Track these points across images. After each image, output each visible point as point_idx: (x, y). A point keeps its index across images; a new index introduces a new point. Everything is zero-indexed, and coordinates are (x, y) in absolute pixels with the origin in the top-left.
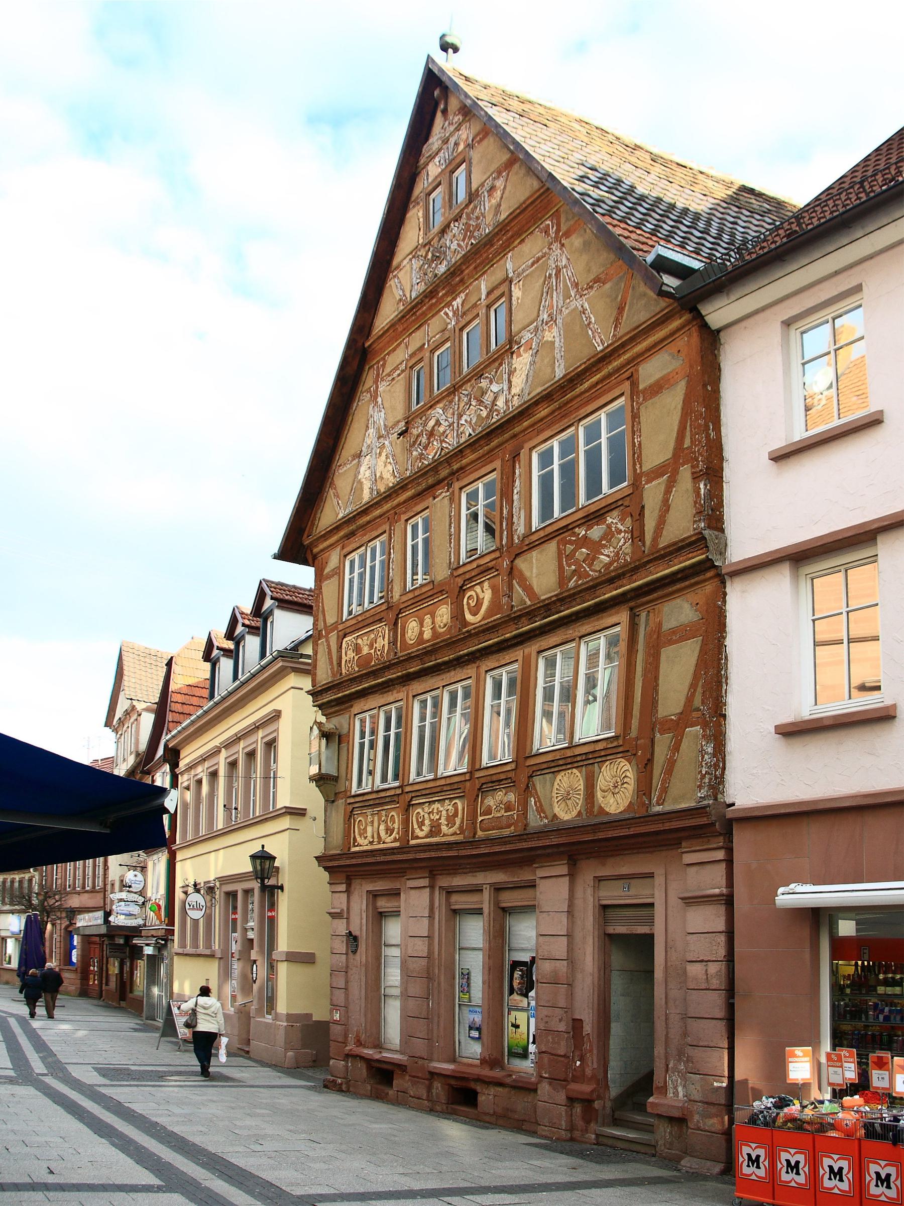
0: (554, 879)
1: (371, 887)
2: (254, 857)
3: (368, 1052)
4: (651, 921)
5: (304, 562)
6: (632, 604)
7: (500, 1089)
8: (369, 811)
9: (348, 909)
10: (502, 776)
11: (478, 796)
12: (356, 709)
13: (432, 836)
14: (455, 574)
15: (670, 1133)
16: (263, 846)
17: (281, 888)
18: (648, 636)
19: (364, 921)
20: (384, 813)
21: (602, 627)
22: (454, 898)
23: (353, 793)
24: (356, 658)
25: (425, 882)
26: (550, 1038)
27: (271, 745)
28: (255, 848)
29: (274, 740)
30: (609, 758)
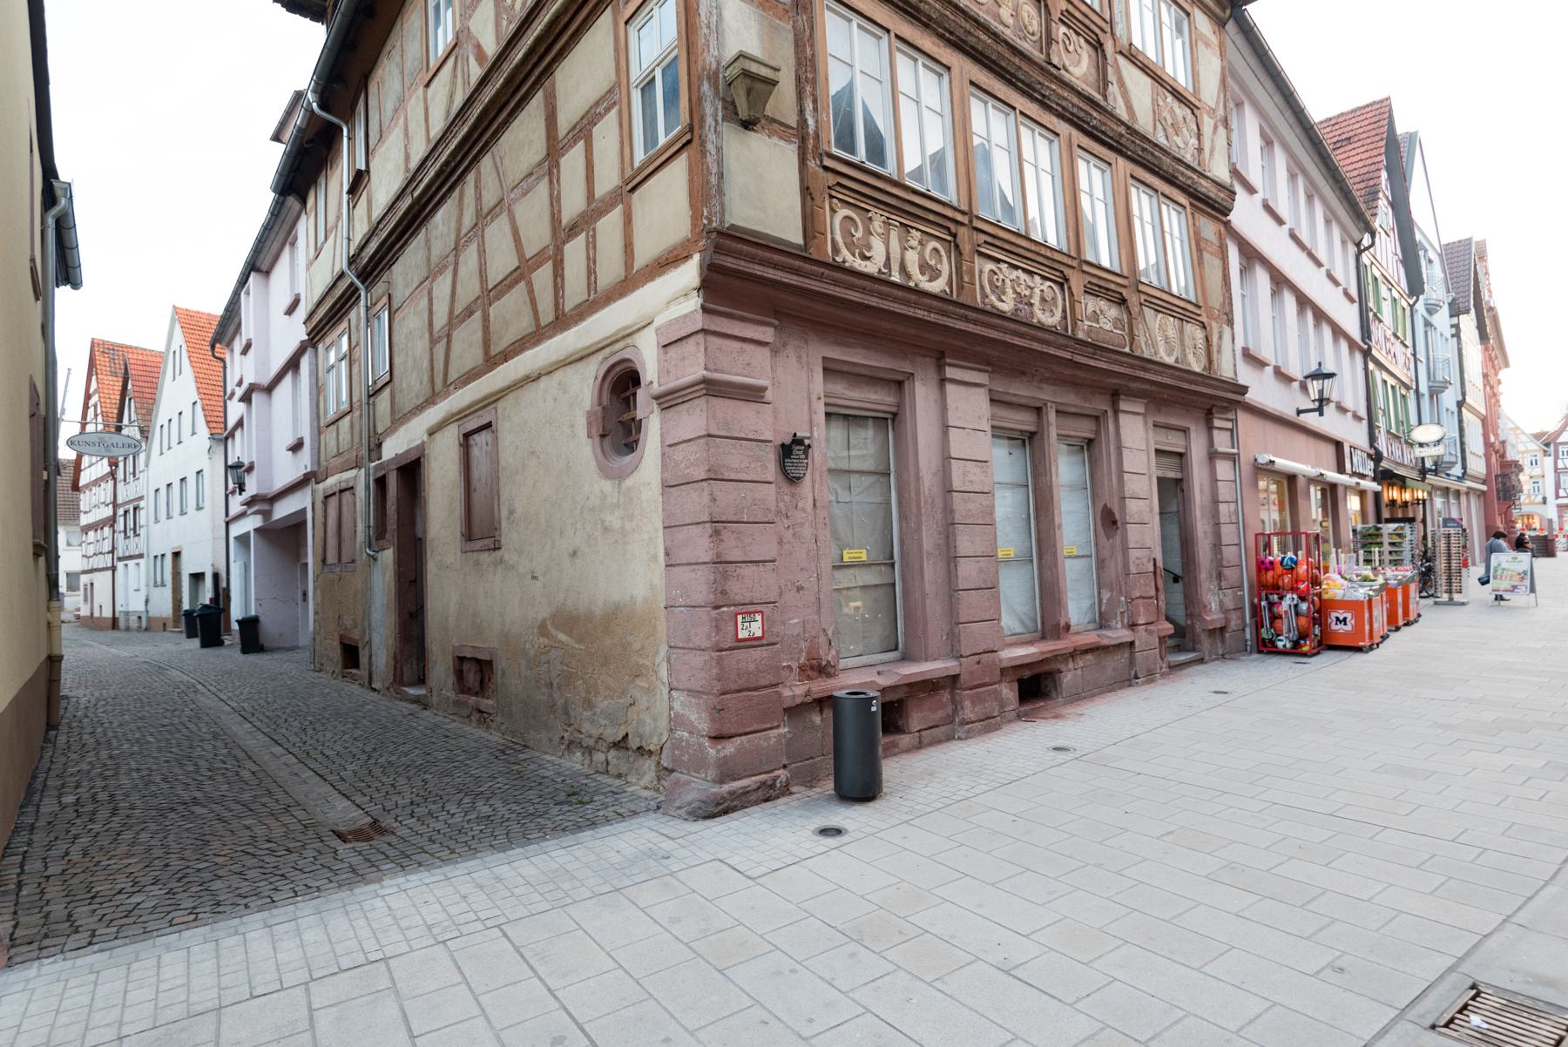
10: (1112, 286)
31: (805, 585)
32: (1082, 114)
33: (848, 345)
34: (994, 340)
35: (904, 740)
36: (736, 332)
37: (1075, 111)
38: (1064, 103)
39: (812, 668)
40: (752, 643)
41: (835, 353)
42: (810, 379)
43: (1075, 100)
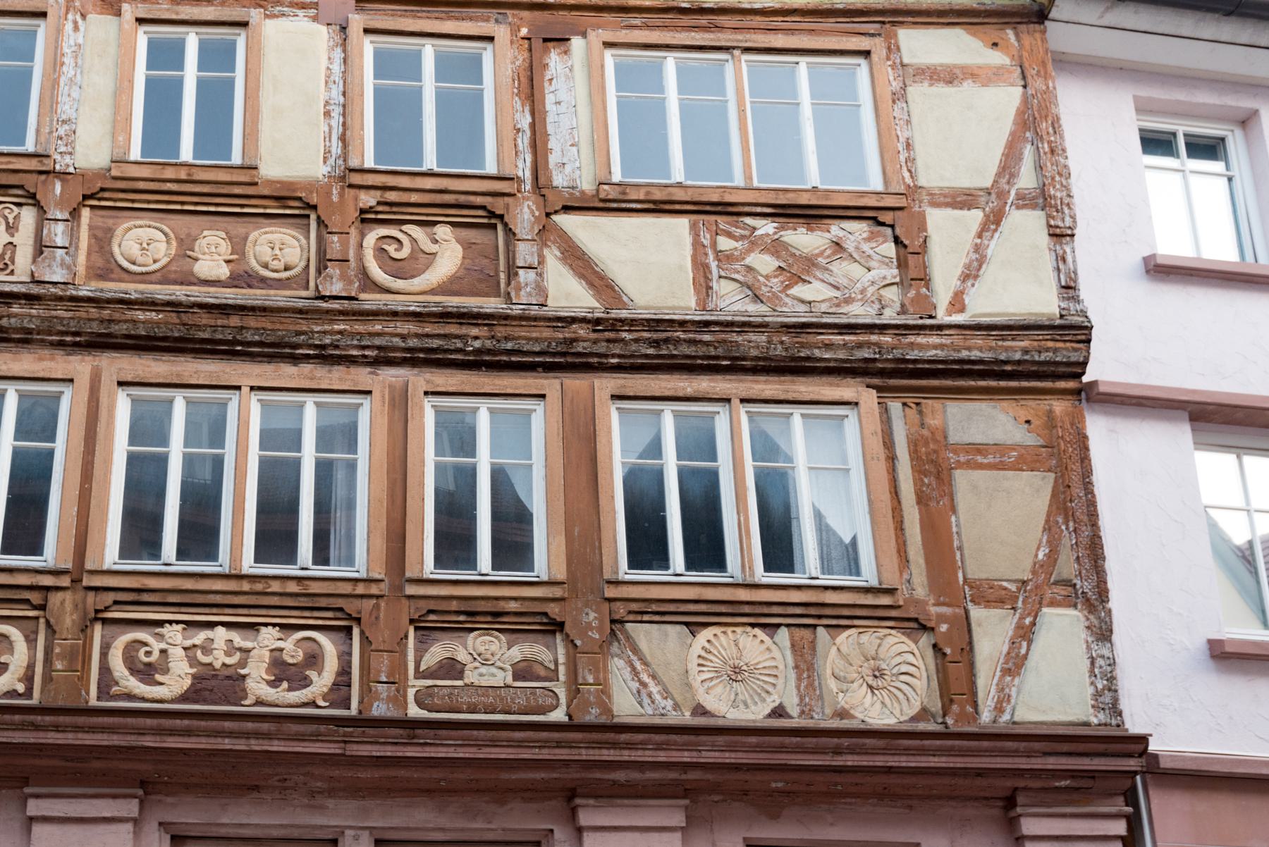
10: (513, 606)
13: (196, 702)
14: (356, 179)
21: (807, 398)
25: (130, 808)
30: (856, 622)
32: (435, 343)
34: (119, 749)
37: (413, 343)
38: (377, 341)
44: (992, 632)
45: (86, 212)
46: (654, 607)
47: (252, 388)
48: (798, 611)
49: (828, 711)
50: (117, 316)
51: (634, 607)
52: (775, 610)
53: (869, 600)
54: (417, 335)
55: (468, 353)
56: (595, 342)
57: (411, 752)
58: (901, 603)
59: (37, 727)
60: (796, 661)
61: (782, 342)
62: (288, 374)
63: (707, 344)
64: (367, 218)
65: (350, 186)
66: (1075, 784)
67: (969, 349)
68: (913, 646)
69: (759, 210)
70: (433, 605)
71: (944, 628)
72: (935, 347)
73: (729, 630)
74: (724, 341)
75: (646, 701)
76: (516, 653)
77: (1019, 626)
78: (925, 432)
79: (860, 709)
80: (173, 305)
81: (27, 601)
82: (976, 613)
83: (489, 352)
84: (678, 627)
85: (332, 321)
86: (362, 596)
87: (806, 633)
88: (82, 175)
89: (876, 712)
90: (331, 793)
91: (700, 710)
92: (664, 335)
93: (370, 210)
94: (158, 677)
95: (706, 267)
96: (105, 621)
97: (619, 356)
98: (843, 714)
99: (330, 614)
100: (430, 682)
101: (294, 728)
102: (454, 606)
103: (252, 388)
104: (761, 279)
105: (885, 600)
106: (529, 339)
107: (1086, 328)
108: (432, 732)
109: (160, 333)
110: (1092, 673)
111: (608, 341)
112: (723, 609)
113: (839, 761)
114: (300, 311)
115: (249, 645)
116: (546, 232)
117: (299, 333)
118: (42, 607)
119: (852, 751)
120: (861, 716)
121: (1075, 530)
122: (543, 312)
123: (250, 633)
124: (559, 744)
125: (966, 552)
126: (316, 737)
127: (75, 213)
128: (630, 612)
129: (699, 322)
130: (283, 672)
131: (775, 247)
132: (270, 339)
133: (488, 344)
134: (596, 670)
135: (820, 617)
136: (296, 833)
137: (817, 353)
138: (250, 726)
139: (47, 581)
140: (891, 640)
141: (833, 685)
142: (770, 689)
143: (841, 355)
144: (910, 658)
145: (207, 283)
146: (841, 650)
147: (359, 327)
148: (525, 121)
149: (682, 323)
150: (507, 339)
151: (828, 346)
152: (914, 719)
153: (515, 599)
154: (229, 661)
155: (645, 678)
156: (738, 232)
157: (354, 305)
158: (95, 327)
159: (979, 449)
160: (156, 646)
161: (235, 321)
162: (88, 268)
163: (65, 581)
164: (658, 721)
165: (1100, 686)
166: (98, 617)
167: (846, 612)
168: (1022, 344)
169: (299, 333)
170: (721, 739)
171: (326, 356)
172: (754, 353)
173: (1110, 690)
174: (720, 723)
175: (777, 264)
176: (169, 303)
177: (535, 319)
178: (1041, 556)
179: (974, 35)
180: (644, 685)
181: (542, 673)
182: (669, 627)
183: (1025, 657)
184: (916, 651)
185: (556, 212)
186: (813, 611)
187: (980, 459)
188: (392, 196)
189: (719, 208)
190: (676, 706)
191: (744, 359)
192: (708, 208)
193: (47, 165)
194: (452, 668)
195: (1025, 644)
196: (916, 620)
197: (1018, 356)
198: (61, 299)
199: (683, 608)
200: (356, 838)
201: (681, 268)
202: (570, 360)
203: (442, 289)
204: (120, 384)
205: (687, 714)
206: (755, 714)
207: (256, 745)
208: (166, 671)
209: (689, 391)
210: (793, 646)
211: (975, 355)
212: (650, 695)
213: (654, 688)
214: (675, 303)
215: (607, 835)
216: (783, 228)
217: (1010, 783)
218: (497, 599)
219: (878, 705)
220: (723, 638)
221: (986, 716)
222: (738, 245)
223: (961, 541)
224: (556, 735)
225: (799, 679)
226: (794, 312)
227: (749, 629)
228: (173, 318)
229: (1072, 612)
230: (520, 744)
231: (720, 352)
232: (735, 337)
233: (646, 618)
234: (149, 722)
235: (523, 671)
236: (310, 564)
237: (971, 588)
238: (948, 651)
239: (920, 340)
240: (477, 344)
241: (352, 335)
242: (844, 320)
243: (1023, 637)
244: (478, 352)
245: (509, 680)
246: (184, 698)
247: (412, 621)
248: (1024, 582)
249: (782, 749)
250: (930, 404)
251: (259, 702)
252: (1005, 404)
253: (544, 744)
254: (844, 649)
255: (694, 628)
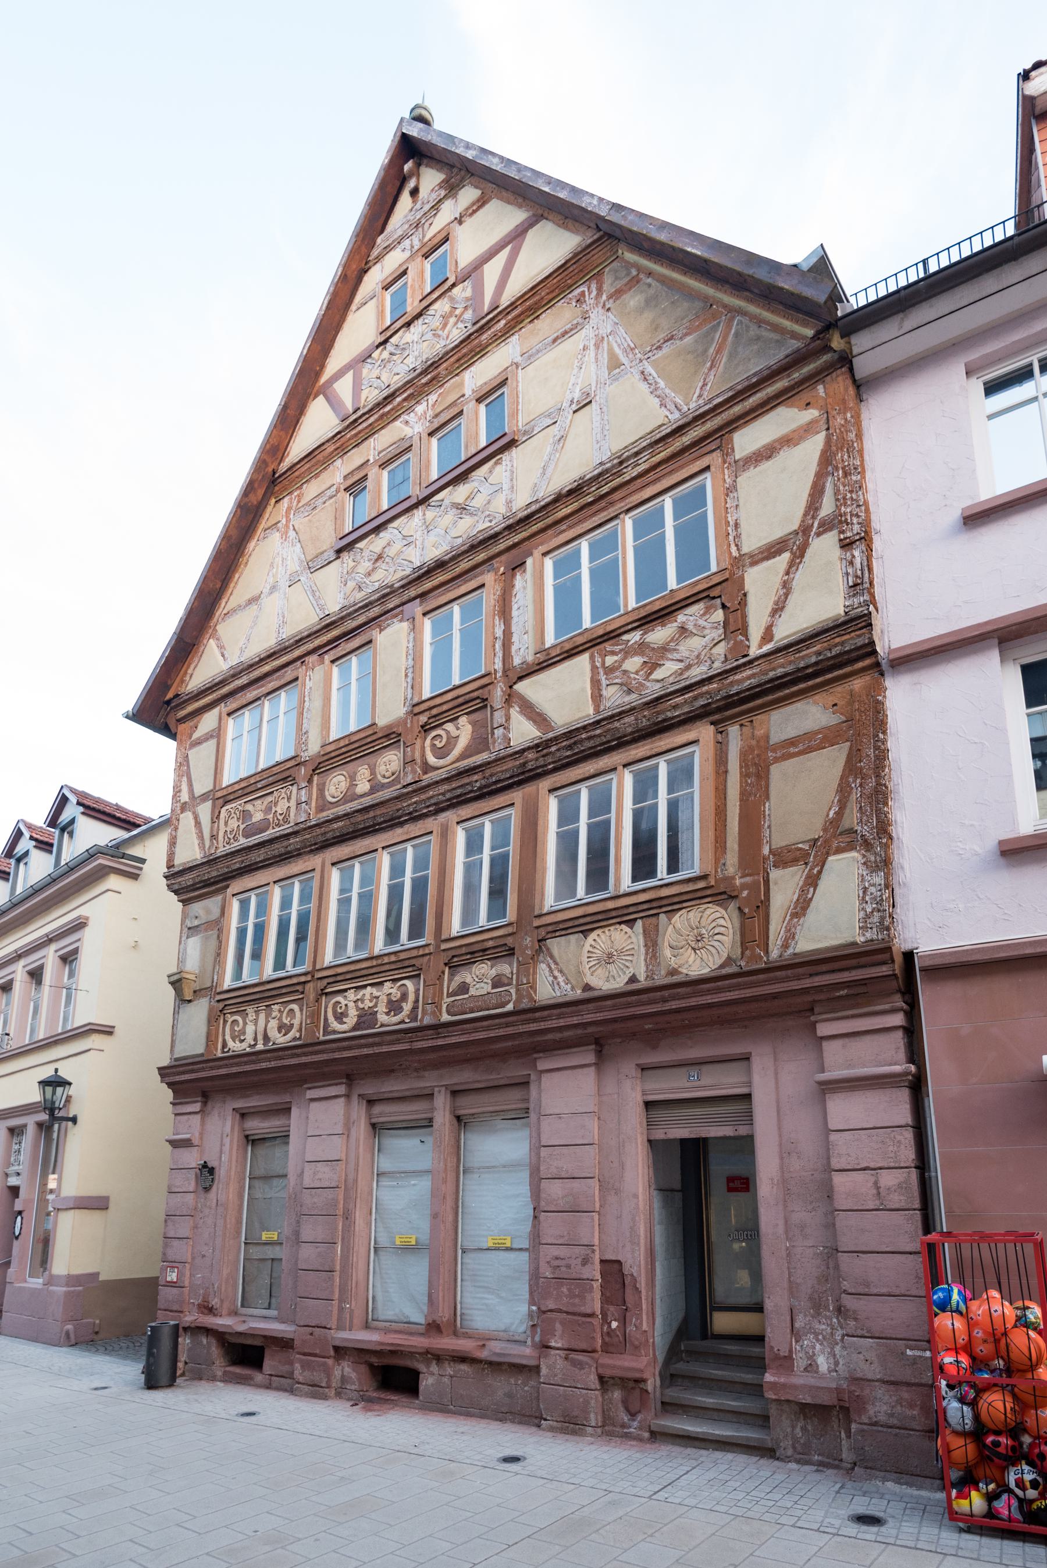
0: (569, 1072)
1: (240, 1104)
2: (44, 1083)
3: (223, 1322)
4: (749, 1117)
5: (167, 730)
6: (717, 717)
7: (464, 1367)
8: (250, 1010)
9: (201, 1134)
10: (491, 944)
11: (443, 972)
12: (230, 891)
13: (358, 1030)
14: (417, 710)
15: (804, 1429)
16: (56, 1070)
17: (74, 1120)
18: (744, 755)
19: (226, 1148)
20: (276, 1007)
21: (664, 748)
22: (377, 1109)
23: (226, 987)
24: (242, 827)
25: (341, 1090)
26: (565, 1290)
27: (68, 959)
28: (47, 1072)
29: (76, 951)
30: (685, 905)
31: (207, 1254)
32: (459, 792)
33: (248, 1096)
35: (259, 1377)
36: (184, 1111)
37: (448, 796)
38: (433, 801)
39: (205, 1307)
40: (172, 1284)
41: (240, 1104)
42: (224, 1126)
43: (446, 787)
44: (784, 886)
45: (316, 778)
46: (561, 926)
47: (383, 848)
48: (645, 906)
49: (663, 973)
50: (327, 829)
51: (550, 928)
52: (632, 909)
53: (691, 887)
54: (449, 791)
55: (475, 791)
56: (537, 759)
57: (440, 1042)
58: (713, 883)
59: (298, 1056)
60: (645, 941)
61: (645, 716)
62: (398, 834)
63: (599, 736)
64: (426, 729)
65: (415, 715)
66: (852, 992)
67: (774, 669)
68: (724, 912)
69: (630, 627)
70: (454, 953)
71: (745, 893)
72: (749, 678)
73: (606, 930)
74: (609, 730)
75: (557, 987)
76: (493, 972)
77: (808, 877)
78: (754, 743)
79: (686, 966)
80: (347, 815)
81: (297, 991)
82: (775, 874)
83: (485, 786)
84: (576, 935)
85: (411, 798)
86: (423, 955)
87: (653, 920)
88: (312, 759)
89: (696, 965)
90: (425, 1069)
91: (587, 988)
92: (572, 741)
93: (426, 724)
94: (345, 1020)
95: (599, 681)
96: (326, 994)
97: (553, 763)
98: (673, 972)
99: (410, 969)
100: (453, 999)
101: (388, 1038)
102: (464, 950)
103: (383, 848)
104: (632, 676)
105: (701, 884)
106: (502, 772)
107: (865, 615)
108: (445, 1030)
109: (345, 831)
110: (863, 900)
111: (543, 756)
112: (600, 917)
113: (667, 1006)
114: (396, 798)
115: (378, 994)
116: (510, 697)
117: (398, 810)
118: (303, 993)
119: (674, 998)
120: (685, 971)
121: (861, 785)
122: (510, 751)
123: (380, 987)
124: (507, 1025)
125: (773, 829)
126: (398, 1041)
127: (310, 781)
128: (548, 933)
129: (593, 723)
130: (394, 1007)
131: (642, 648)
132: (387, 818)
133: (483, 782)
134: (527, 976)
135: (660, 907)
136: (416, 1093)
137: (669, 714)
138: (371, 1040)
139: (303, 979)
140: (708, 912)
141: (668, 952)
142: (627, 964)
143: (686, 709)
144: (722, 922)
145: (362, 796)
146: (677, 927)
147: (423, 797)
148: (499, 632)
149: (584, 727)
150: (491, 776)
151: (675, 707)
152: (722, 966)
153: (491, 939)
154: (371, 1005)
155: (556, 973)
156: (617, 648)
157: (419, 785)
158: (321, 839)
159: (792, 742)
160: (343, 1002)
161: (372, 814)
162: (316, 807)
163: (309, 978)
164: (561, 1000)
165: (869, 910)
166: (323, 993)
167: (676, 899)
168: (815, 649)
169: (398, 810)
170: (591, 1006)
171: (415, 817)
172: (629, 730)
173: (879, 911)
174: (596, 994)
175: (643, 660)
176: (345, 815)
177: (503, 758)
178: (831, 816)
179: (791, 406)
180: (555, 978)
181: (506, 981)
182: (571, 937)
183: (811, 899)
184: (726, 916)
185: (515, 683)
186: (655, 904)
187: (792, 750)
188: (434, 712)
189: (605, 638)
190: (573, 989)
191: (625, 736)
192: (599, 640)
193: (298, 760)
194: (464, 988)
195: (812, 890)
196: (725, 893)
197: (813, 659)
198: (305, 829)
199: (577, 922)
200: (440, 1092)
201: (583, 690)
202: (527, 775)
203: (463, 756)
204: (333, 864)
205: (579, 992)
206: (618, 983)
207: (377, 1050)
208: (347, 1016)
209: (592, 771)
210: (644, 931)
211: (780, 671)
212: (558, 984)
213: (561, 979)
214: (580, 715)
215: (553, 1074)
216: (645, 633)
217: (810, 998)
218: (483, 941)
219: (698, 961)
220: (603, 936)
221: (774, 953)
222: (616, 658)
223: (770, 820)
224: (503, 1020)
225: (647, 954)
226: (653, 689)
227: (618, 926)
228: (348, 822)
229: (854, 854)
230: (488, 1029)
231: (609, 737)
232: (617, 724)
233: (557, 934)
234: (334, 1045)
235: (497, 982)
236: (406, 942)
237: (774, 855)
238: (746, 910)
239: (738, 677)
240: (478, 784)
241: (421, 802)
242: (683, 684)
243: (810, 885)
244: (480, 788)
245: (489, 989)
246: (354, 1029)
247: (446, 964)
248: (816, 840)
249: (629, 1005)
250: (758, 719)
251: (382, 1025)
252: (817, 697)
253: (500, 1026)
254: (678, 925)
255: (585, 933)
